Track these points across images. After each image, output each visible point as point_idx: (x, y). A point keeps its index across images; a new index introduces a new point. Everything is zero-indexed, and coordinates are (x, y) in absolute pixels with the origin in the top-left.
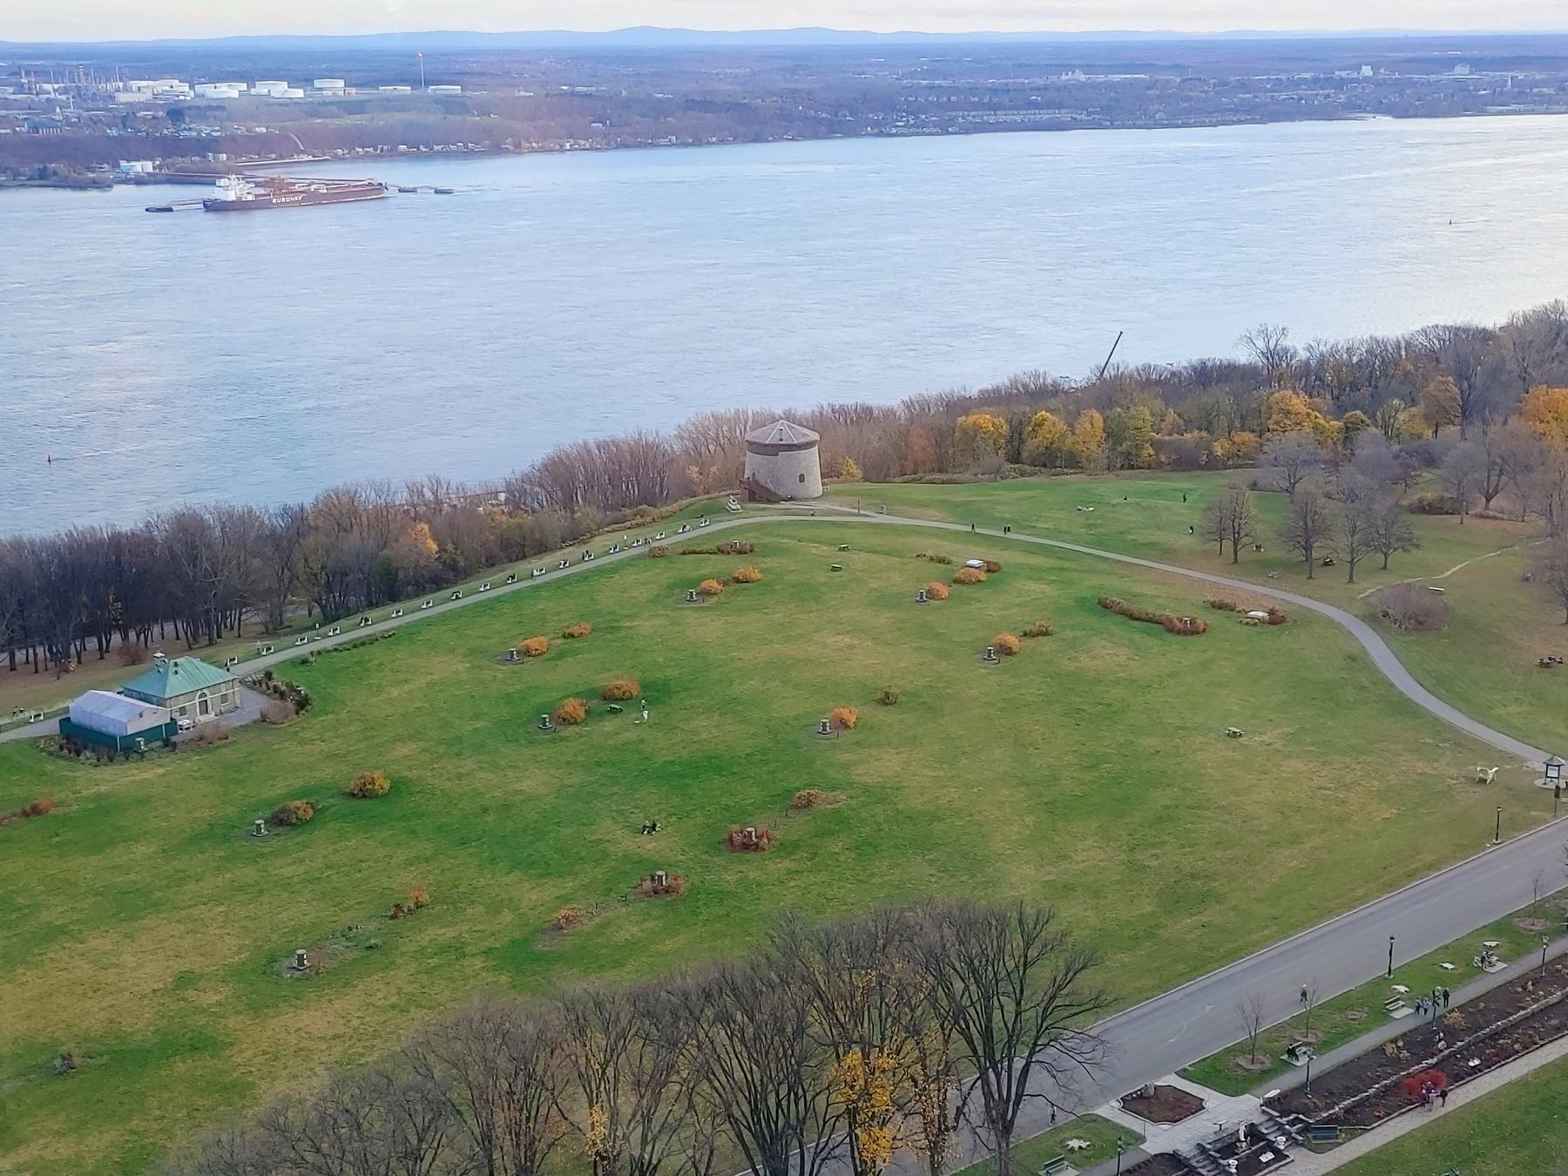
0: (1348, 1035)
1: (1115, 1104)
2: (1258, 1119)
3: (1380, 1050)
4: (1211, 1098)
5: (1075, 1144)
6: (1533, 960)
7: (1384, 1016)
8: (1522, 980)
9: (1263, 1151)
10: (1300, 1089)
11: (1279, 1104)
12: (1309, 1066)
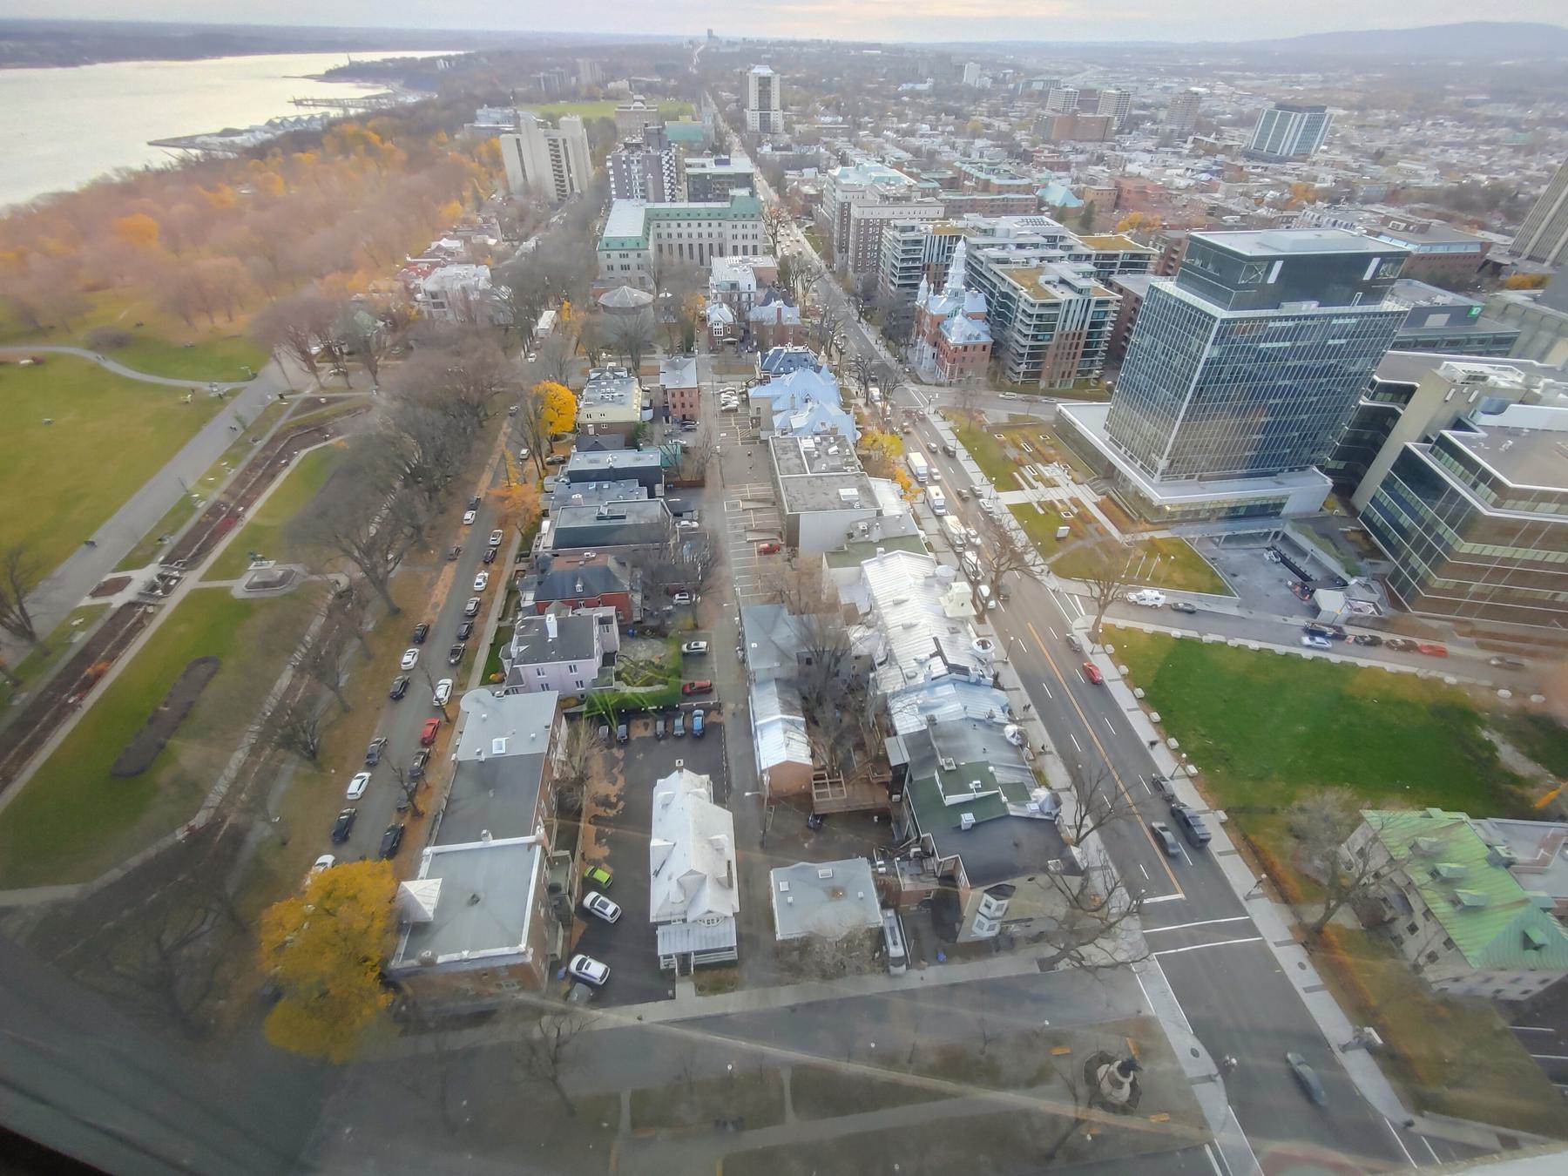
0: (181, 523)
1: (87, 598)
2: (160, 571)
3: (199, 522)
4: (133, 574)
5: (76, 623)
6: (244, 464)
7: (193, 509)
8: (244, 472)
9: (170, 581)
10: (173, 551)
11: (169, 560)
12: (171, 542)
